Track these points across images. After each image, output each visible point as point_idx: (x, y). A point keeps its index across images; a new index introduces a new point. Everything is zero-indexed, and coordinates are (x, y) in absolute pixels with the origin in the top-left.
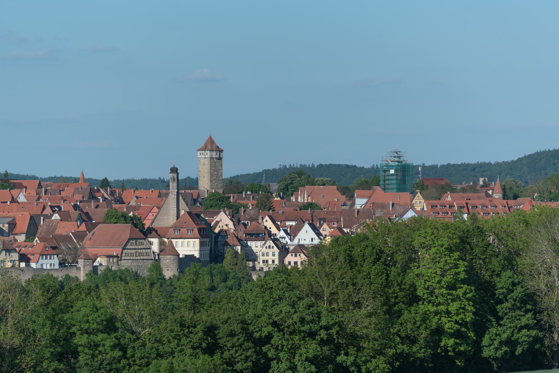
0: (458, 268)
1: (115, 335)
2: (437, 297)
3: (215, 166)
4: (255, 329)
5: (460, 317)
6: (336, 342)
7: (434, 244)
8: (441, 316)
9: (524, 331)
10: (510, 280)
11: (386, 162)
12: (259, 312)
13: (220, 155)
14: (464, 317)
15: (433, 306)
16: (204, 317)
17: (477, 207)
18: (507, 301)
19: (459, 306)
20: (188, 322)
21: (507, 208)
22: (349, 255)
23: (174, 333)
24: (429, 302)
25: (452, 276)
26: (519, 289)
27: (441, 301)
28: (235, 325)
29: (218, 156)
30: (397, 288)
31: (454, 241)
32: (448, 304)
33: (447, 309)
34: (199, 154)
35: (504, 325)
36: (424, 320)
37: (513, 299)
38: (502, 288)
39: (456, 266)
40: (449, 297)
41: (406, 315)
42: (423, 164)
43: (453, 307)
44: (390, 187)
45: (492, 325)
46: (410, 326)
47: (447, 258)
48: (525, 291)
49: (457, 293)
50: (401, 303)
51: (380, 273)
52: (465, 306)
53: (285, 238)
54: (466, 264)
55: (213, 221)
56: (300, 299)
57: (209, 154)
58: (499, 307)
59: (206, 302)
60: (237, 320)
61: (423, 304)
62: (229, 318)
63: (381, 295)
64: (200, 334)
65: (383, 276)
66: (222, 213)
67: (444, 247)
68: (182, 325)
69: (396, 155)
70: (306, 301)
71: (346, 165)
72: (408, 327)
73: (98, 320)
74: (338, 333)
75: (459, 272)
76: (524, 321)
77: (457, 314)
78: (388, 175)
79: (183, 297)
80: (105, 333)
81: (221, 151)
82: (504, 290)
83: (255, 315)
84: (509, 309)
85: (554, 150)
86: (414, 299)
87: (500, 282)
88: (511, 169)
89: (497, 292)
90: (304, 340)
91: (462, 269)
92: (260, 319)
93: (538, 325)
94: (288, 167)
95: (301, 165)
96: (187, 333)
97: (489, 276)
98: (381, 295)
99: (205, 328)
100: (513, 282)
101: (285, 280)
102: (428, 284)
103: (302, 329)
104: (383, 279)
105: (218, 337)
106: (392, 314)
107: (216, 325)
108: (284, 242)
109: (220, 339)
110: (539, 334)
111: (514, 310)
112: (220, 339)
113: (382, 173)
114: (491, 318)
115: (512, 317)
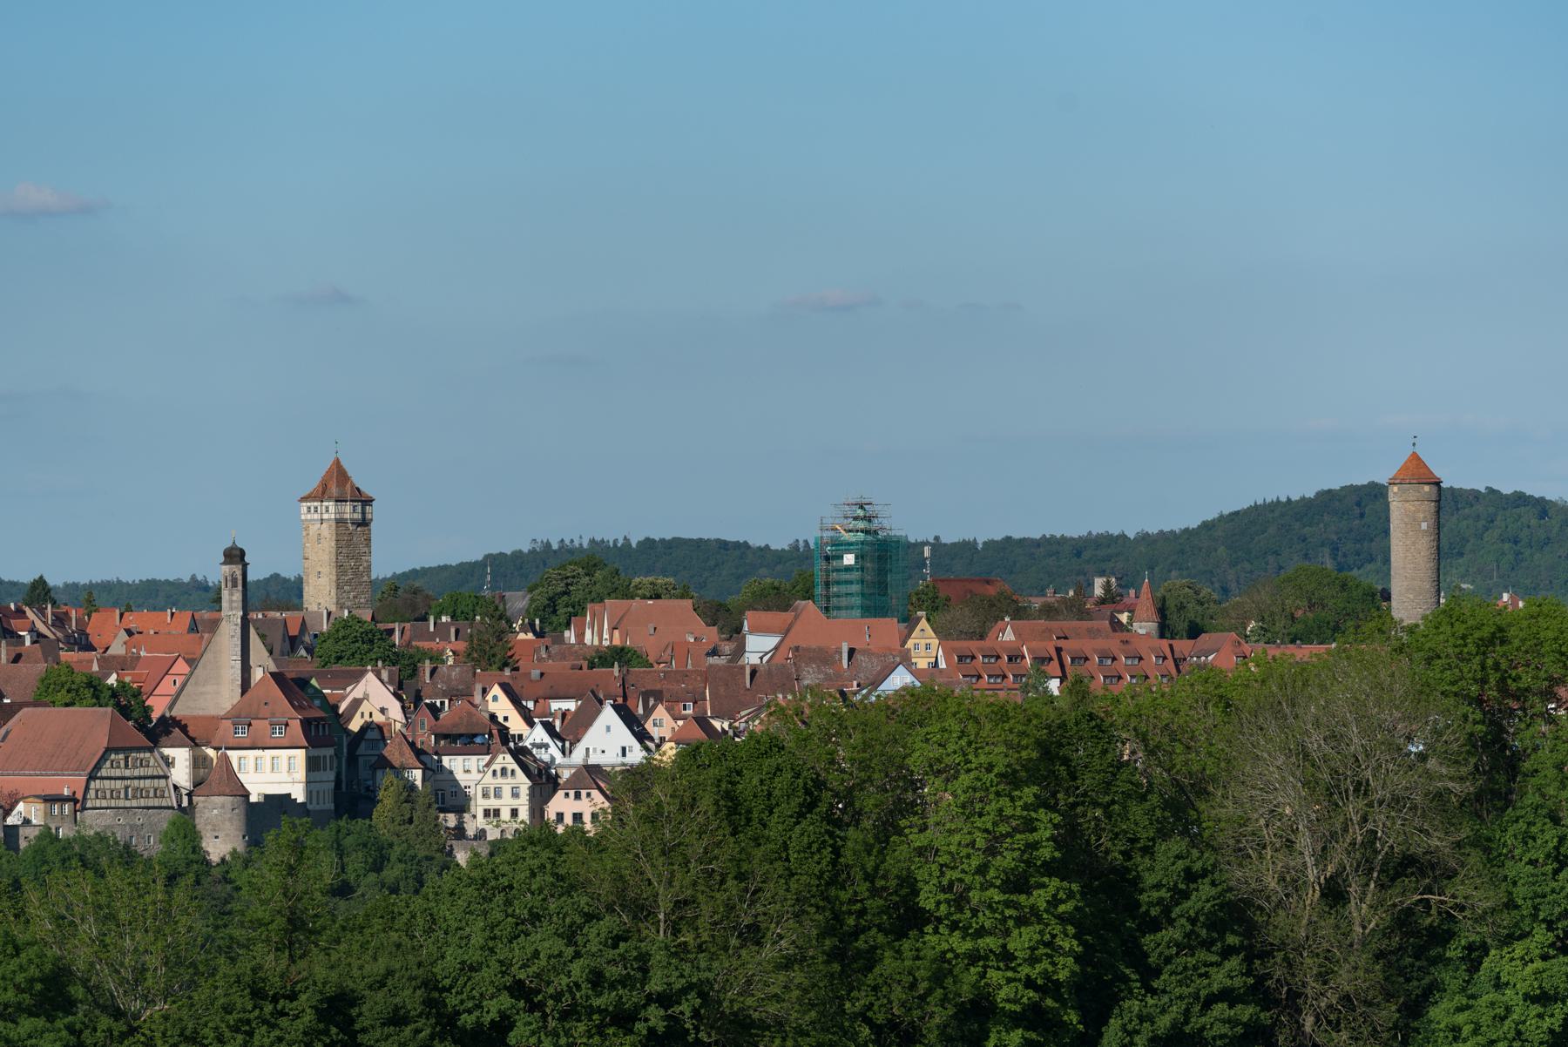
0: (1034, 830)
1: (66, 1021)
2: (975, 912)
3: (349, 543)
4: (462, 1002)
5: (1039, 968)
6: (690, 1038)
7: (968, 762)
8: (985, 967)
9: (1220, 1009)
10: (1180, 864)
11: (831, 534)
12: (475, 956)
13: (363, 513)
14: (1050, 969)
15: (964, 938)
16: (319, 971)
17: (1086, 659)
18: (1171, 922)
19: (1037, 937)
20: (275, 984)
21: (1170, 663)
22: (728, 796)
23: (235, 1016)
24: (954, 926)
25: (1017, 853)
26: (1205, 889)
27: (987, 924)
28: (407, 992)
29: (358, 516)
30: (863, 888)
31: (1024, 754)
32: (1007, 933)
33: (1004, 946)
35: (1164, 991)
36: (938, 978)
37: (1189, 919)
38: (1158, 886)
39: (1030, 826)
40: (1008, 912)
41: (888, 964)
42: (937, 538)
43: (1021, 940)
44: (844, 602)
45: (1131, 992)
46: (898, 993)
47: (1004, 802)
48: (1221, 894)
49: (1032, 900)
50: (874, 930)
51: (815, 847)
52: (1054, 936)
54: (1057, 818)
55: (344, 698)
56: (590, 917)
57: (332, 509)
58: (1148, 941)
59: (324, 928)
60: (411, 979)
61: (936, 931)
62: (390, 973)
63: (818, 907)
64: (308, 1017)
65: (825, 852)
66: (370, 676)
67: (996, 770)
68: (257, 994)
69: (860, 513)
70: (608, 924)
71: (718, 540)
72: (893, 997)
73: (20, 978)
74: (696, 1014)
75: (1037, 843)
76: (1219, 979)
77: (1033, 960)
78: (838, 570)
79: (260, 914)
80: (38, 1016)
81: (368, 502)
82: (1163, 893)
83: (463, 963)
84: (1177, 945)
85: (1303, 499)
86: (910, 919)
87: (1151, 869)
88: (1182, 552)
89: (1144, 898)
90: (601, 1034)
91: (1045, 833)
92: (477, 976)
93: (1259, 993)
94: (555, 546)
95: (592, 541)
96: (272, 1014)
97: (1121, 852)
98: (818, 907)
99: (321, 1001)
100: (1188, 870)
101: (549, 866)
102: (950, 875)
103: (597, 1002)
104: (824, 862)
105: (357, 1027)
106: (849, 960)
107: (353, 991)
109: (364, 1030)
110: (1262, 1016)
111: (1192, 950)
112: (364, 1030)
113: (820, 565)
114: (1127, 971)
115: (1186, 968)
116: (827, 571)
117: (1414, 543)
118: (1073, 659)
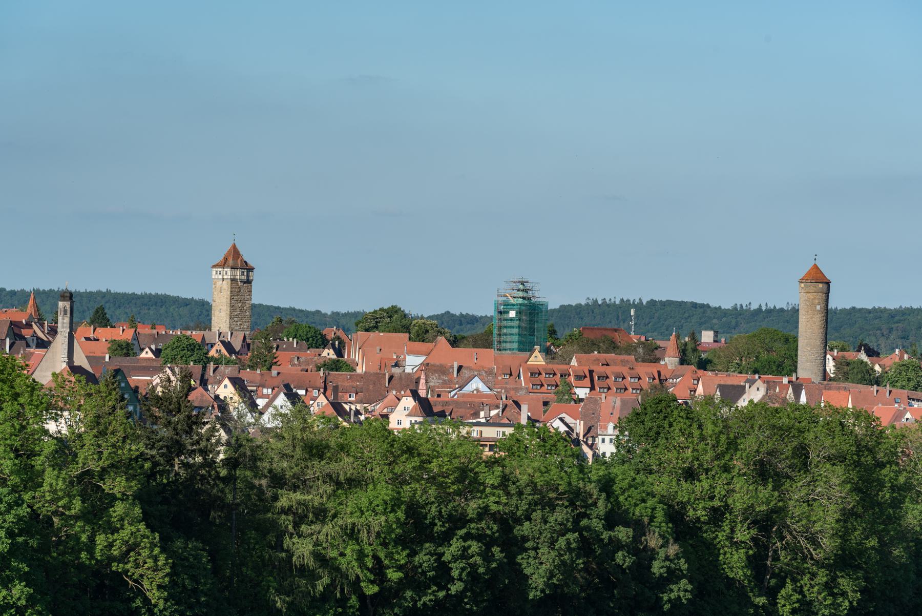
11: (504, 299)
13: (248, 276)
17: (607, 377)
21: (657, 381)
29: (244, 278)
34: (214, 273)
44: (509, 338)
57: (229, 273)
69: (521, 287)
71: (692, 303)
81: (251, 269)
94: (618, 302)
95: (622, 300)
116: (500, 320)
117: (812, 318)
118: (599, 378)
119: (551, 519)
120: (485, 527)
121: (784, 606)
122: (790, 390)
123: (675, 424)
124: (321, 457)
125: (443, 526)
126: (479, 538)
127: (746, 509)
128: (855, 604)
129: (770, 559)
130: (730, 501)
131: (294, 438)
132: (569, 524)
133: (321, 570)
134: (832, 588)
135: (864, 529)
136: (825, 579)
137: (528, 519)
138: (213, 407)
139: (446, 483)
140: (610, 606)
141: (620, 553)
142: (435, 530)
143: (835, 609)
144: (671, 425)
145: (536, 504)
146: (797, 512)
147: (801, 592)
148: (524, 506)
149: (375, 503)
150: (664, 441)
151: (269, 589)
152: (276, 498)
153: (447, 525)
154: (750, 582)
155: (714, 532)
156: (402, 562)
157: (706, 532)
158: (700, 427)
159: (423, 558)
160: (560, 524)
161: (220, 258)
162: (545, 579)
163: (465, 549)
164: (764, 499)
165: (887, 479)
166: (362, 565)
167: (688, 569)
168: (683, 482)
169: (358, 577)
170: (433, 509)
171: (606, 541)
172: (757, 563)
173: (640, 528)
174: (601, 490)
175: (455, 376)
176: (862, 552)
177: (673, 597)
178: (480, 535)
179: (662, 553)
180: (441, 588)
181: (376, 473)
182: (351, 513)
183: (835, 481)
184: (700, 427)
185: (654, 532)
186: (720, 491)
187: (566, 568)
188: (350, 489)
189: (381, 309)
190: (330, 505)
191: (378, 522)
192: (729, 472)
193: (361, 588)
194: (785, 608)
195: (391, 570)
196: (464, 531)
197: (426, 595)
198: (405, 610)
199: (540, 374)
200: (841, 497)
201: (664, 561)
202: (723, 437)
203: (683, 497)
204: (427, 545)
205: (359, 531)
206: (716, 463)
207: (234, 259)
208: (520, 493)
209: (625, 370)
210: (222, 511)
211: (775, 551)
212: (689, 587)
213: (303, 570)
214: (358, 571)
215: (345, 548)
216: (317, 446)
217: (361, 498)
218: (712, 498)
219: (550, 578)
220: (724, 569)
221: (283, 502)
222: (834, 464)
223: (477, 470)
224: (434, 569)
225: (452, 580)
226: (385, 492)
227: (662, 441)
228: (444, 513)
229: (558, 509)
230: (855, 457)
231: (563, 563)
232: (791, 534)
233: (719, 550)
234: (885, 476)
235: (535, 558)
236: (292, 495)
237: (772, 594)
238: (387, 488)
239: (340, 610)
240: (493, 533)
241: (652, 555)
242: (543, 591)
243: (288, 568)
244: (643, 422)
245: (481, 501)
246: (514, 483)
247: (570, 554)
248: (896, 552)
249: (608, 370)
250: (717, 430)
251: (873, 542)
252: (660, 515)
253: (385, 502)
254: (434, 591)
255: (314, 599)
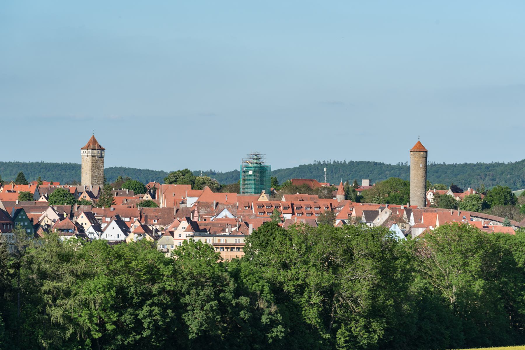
3: (96, 164)
11: (246, 164)
13: (101, 154)
17: (302, 207)
21: (330, 209)
34: (82, 152)
42: (444, 163)
44: (249, 186)
53: (93, 233)
55: (41, 215)
57: (91, 152)
66: (50, 209)
69: (255, 157)
81: (103, 150)
88: (512, 169)
94: (332, 163)
95: (334, 161)
108: (93, 237)
113: (242, 174)
117: (417, 171)
118: (297, 208)
119: (202, 294)
120: (162, 299)
121: (340, 339)
122: (405, 212)
123: (276, 238)
124: (68, 261)
125: (138, 299)
126: (160, 304)
127: (316, 285)
128: (381, 337)
129: (333, 313)
130: (307, 280)
131: (51, 251)
132: (212, 296)
133: (68, 325)
134: (368, 328)
135: (386, 295)
136: (363, 323)
137: (189, 293)
138: (75, 229)
139: (140, 275)
140: (237, 342)
141: (242, 312)
142: (134, 301)
143: (370, 340)
144: (274, 239)
145: (193, 285)
146: (346, 286)
147: (350, 331)
148: (185, 287)
149: (98, 287)
150: (270, 248)
151: (38, 336)
152: (42, 285)
153: (140, 298)
154: (320, 326)
155: (298, 298)
156: (115, 319)
157: (295, 298)
158: (290, 240)
159: (127, 317)
160: (207, 296)
161: (85, 144)
162: (198, 327)
163: (151, 311)
164: (326, 279)
165: (399, 266)
166: (91, 321)
167: (282, 319)
168: (281, 271)
169: (89, 328)
170: (132, 289)
171: (234, 305)
172: (325, 315)
173: (254, 297)
174: (231, 276)
175: (214, 208)
176: (384, 308)
177: (274, 336)
178: (160, 303)
179: (267, 311)
180: (138, 334)
181: (99, 270)
182: (85, 293)
183: (368, 268)
184: (290, 240)
185: (263, 299)
186: (302, 275)
187: (211, 322)
188: (84, 279)
189: (179, 171)
190: (73, 288)
191: (100, 298)
192: (307, 264)
193: (91, 335)
194: (341, 341)
195: (108, 324)
196: (151, 301)
197: (129, 337)
198: (117, 346)
199: (263, 206)
200: (371, 277)
201: (268, 315)
202: (303, 245)
203: (281, 279)
204: (129, 309)
205: (89, 303)
206: (299, 259)
207: (94, 144)
208: (184, 279)
209: (311, 203)
210: (10, 293)
211: (335, 308)
212: (283, 330)
213: (57, 325)
214: (89, 325)
215: (82, 312)
216: (66, 255)
217: (90, 284)
218: (298, 279)
219: (200, 327)
220: (305, 319)
221: (45, 287)
222: (367, 259)
223: (159, 267)
224: (133, 323)
225: (144, 329)
226: (104, 280)
227: (269, 248)
228: (138, 292)
229: (206, 287)
230: (381, 255)
231: (208, 318)
232: (342, 298)
233: (302, 308)
234: (398, 265)
235: (192, 316)
236: (51, 283)
237: (334, 332)
238: (105, 278)
239: (80, 347)
240: (168, 302)
241: (261, 312)
242: (197, 334)
243: (49, 325)
244: (259, 237)
245: (160, 285)
246: (180, 274)
247: (213, 313)
248: (405, 307)
249: (302, 203)
250: (300, 241)
251: (391, 302)
252: (266, 289)
253: (104, 286)
254: (134, 335)
255: (64, 341)
